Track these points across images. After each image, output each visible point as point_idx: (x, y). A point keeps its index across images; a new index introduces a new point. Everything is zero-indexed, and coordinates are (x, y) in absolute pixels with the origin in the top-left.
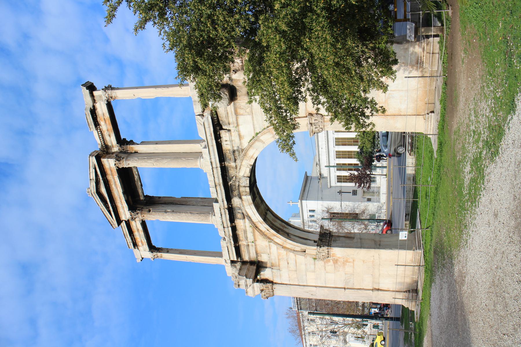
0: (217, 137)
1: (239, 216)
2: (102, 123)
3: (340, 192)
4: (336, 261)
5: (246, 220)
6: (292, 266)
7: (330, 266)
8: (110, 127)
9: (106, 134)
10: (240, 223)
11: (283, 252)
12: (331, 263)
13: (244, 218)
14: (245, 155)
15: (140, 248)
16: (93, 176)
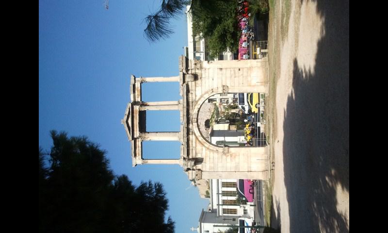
0: (187, 95)
1: (190, 133)
2: (136, 92)
3: (225, 219)
4: (231, 156)
5: (194, 135)
6: (212, 160)
7: (229, 158)
8: (139, 94)
9: (136, 96)
10: (191, 136)
11: (208, 152)
12: (229, 156)
13: (192, 134)
14: (197, 103)
15: (137, 158)
16: (127, 113)
